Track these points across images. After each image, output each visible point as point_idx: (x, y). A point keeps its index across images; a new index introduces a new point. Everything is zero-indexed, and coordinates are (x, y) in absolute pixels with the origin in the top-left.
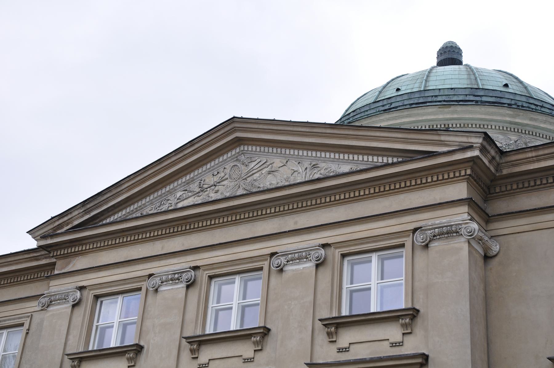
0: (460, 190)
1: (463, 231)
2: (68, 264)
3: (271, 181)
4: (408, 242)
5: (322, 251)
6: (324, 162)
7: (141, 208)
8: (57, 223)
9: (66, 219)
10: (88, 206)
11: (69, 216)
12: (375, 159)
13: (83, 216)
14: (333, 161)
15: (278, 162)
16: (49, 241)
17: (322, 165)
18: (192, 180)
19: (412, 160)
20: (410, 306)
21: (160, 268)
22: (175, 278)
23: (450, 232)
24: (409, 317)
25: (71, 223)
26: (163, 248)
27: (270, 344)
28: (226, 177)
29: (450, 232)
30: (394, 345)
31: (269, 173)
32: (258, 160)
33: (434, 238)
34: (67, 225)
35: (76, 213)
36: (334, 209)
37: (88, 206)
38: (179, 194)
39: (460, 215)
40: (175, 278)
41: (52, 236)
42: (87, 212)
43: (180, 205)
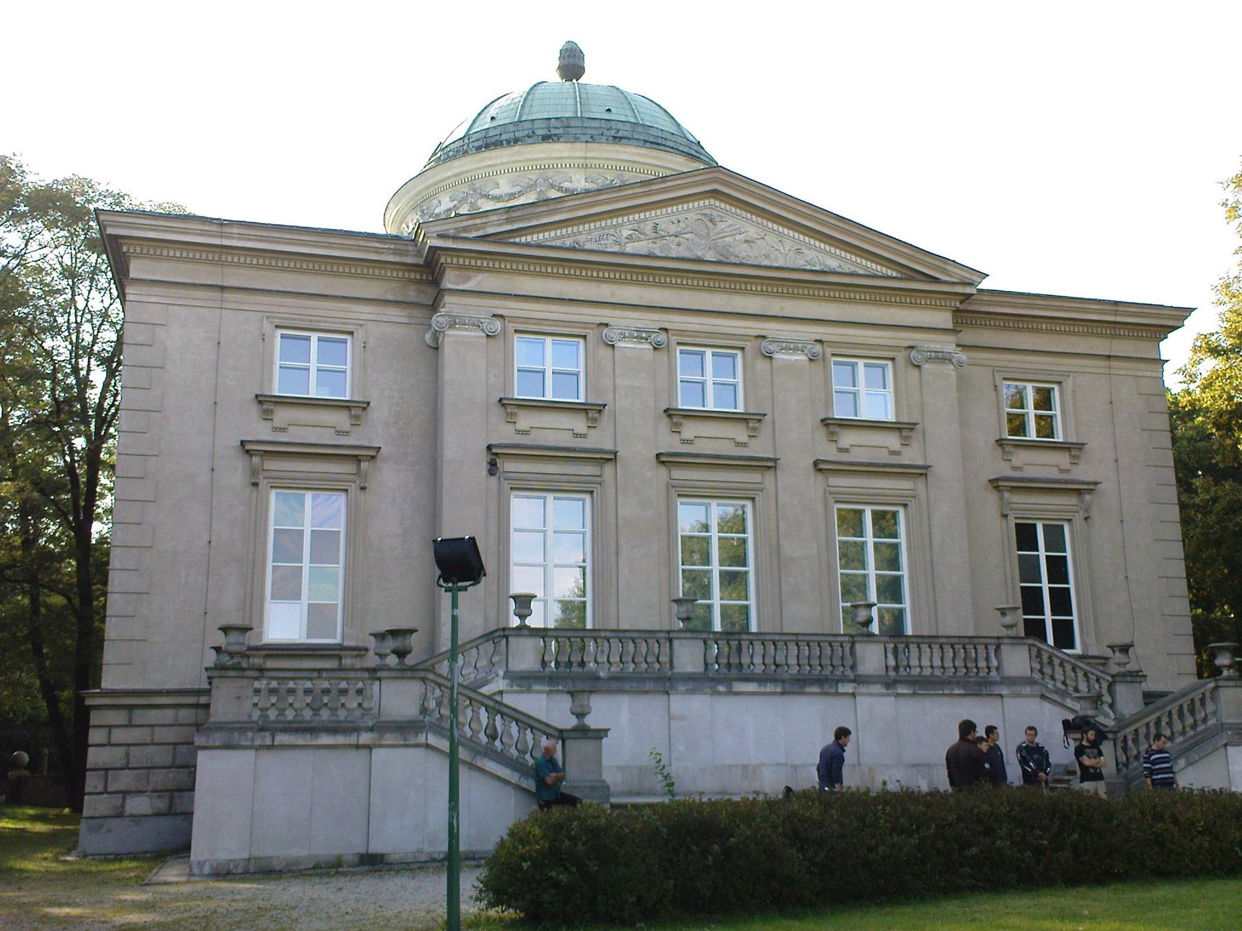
0: (943, 319)
1: (954, 360)
2: (469, 279)
3: (744, 252)
4: (901, 357)
5: (818, 348)
6: (809, 249)
7: (574, 234)
8: (465, 224)
9: (478, 221)
10: (514, 214)
11: (484, 220)
12: (879, 267)
13: (501, 225)
14: (820, 251)
15: (752, 232)
16: (449, 244)
17: (807, 252)
18: (646, 220)
19: (911, 279)
20: (906, 420)
21: (622, 320)
22: (640, 335)
23: (944, 359)
24: (901, 428)
25: (484, 228)
26: (612, 295)
27: (765, 429)
28: (689, 229)
29: (944, 359)
30: (893, 453)
31: (746, 241)
32: (730, 222)
33: (929, 360)
34: (478, 230)
35: (495, 218)
36: (823, 304)
37: (514, 214)
38: (626, 233)
39: (946, 344)
40: (640, 335)
41: (454, 238)
42: (509, 221)
43: (629, 248)
